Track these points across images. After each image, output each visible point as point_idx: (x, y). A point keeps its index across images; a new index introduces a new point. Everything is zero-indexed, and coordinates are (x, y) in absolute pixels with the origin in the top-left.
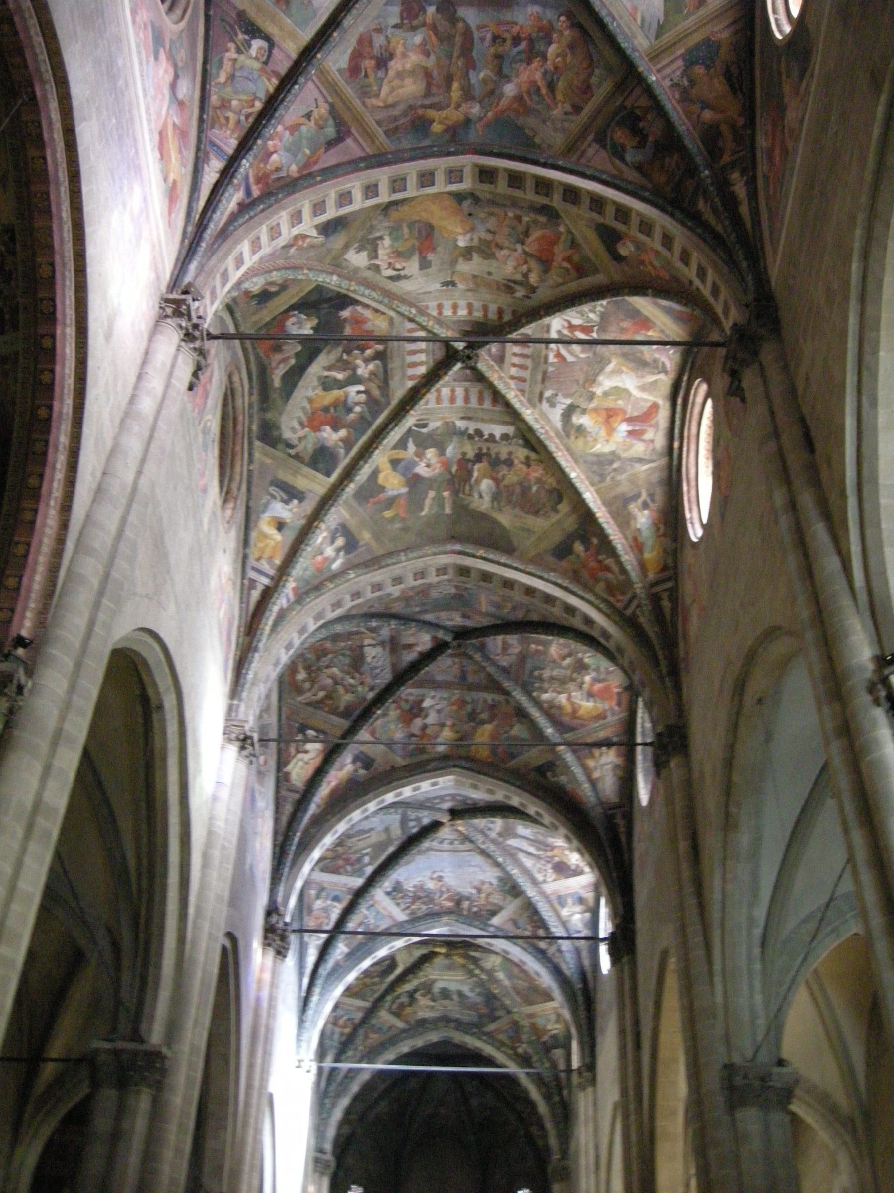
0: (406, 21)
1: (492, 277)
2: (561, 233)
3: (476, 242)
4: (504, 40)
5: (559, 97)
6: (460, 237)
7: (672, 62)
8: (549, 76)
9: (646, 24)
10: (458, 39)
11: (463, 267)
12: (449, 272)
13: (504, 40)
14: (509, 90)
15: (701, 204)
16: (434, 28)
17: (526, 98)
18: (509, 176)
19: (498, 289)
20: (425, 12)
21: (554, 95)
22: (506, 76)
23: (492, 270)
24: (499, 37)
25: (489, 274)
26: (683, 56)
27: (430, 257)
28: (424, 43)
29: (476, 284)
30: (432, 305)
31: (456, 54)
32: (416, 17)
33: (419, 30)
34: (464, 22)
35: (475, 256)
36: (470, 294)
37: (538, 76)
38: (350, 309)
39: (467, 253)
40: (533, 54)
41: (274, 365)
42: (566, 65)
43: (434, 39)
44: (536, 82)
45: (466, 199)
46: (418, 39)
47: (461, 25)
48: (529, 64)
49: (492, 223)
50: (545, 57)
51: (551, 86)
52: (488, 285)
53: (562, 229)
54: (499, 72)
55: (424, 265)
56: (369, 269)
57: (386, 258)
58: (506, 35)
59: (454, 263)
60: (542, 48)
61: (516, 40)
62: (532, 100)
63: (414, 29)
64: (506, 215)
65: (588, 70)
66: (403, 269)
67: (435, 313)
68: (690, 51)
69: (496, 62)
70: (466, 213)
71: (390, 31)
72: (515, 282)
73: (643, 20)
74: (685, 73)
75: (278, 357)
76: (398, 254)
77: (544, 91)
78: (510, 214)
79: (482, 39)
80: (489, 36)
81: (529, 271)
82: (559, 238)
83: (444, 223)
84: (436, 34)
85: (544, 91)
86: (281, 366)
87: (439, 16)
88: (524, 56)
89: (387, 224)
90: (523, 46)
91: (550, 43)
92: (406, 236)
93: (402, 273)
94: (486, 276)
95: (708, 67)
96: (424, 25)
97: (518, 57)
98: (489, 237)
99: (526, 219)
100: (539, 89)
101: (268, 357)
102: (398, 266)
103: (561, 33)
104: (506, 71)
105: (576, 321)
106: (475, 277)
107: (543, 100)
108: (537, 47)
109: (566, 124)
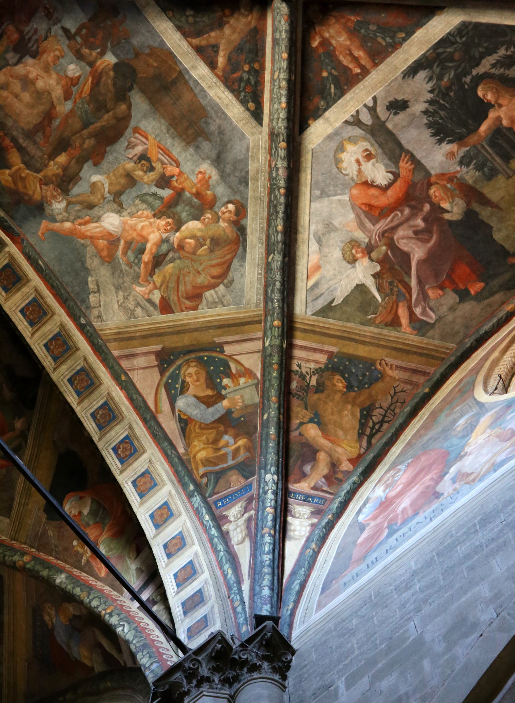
0: (79, 40)
4: (152, 169)
5: (157, 278)
7: (315, 350)
8: (164, 248)
9: (317, 292)
10: (107, 119)
13: (152, 169)
14: (111, 221)
15: (234, 512)
16: (97, 78)
17: (122, 243)
18: (35, 300)
20: (102, 54)
21: (152, 274)
22: (121, 205)
24: (149, 160)
26: (331, 355)
28: (74, 82)
31: (92, 128)
32: (91, 47)
33: (83, 64)
34: (129, 107)
37: (154, 237)
40: (169, 209)
42: (194, 253)
43: (87, 88)
44: (146, 241)
46: (73, 69)
47: (124, 107)
48: (154, 216)
50: (178, 225)
51: (158, 261)
54: (117, 195)
58: (158, 166)
60: (184, 215)
61: (164, 181)
62: (125, 253)
63: (80, 56)
65: (213, 281)
68: (342, 356)
69: (123, 181)
71: (56, 29)
73: (316, 285)
74: (318, 371)
77: (146, 257)
79: (131, 146)
80: (139, 149)
84: (92, 89)
85: (146, 257)
87: (112, 73)
88: (157, 204)
90: (166, 193)
91: (196, 218)
95: (349, 387)
96: (91, 64)
97: (150, 199)
100: (142, 251)
103: (217, 219)
104: (124, 198)
107: (138, 264)
108: (179, 208)
109: (139, 310)
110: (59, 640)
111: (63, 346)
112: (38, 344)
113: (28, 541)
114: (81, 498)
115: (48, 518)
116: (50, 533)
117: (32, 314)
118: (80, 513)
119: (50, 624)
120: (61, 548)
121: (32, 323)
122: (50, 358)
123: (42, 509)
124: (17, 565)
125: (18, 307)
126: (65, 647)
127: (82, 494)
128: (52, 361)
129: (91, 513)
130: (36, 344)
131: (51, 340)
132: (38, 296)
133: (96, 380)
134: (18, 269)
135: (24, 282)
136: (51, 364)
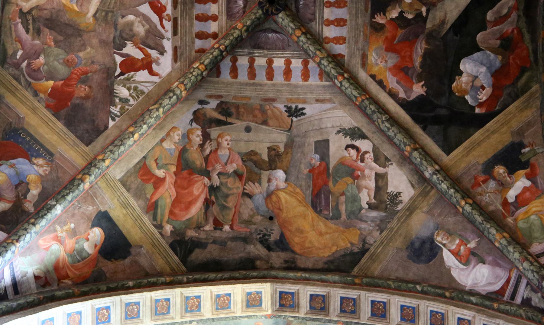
1: (244, 124)
2: (168, 222)
3: (265, 174)
6: (282, 185)
11: (279, 138)
12: (294, 131)
19: (237, 107)
23: (244, 135)
25: (248, 130)
27: (316, 159)
29: (263, 112)
30: (314, 80)
35: (265, 157)
36: (270, 95)
38: (413, 96)
39: (275, 159)
41: (514, 15)
45: (276, 242)
49: (247, 208)
52: (250, 110)
53: (168, 228)
55: (323, 147)
56: (387, 159)
57: (367, 172)
59: (290, 145)
64: (231, 228)
66: (348, 147)
67: (312, 65)
70: (275, 220)
72: (219, 123)
75: (507, 27)
76: (352, 172)
78: (227, 228)
81: (202, 146)
82: (171, 213)
83: (301, 209)
86: (505, 11)
89: (363, 226)
92: (343, 198)
93: (348, 141)
94: (252, 125)
98: (251, 187)
99: (208, 227)
101: (520, 32)
102: (353, 152)
105: (142, 75)
106: (265, 123)
110: (21, 160)
111: (191, 309)
112: (203, 293)
113: (96, 186)
114: (96, 246)
115: (100, 211)
116: (91, 208)
117: (222, 301)
118: (88, 240)
119: (35, 161)
120: (76, 211)
121: (218, 296)
122: (190, 295)
123: (108, 211)
124: (87, 176)
125: (234, 294)
126: (13, 161)
127: (98, 248)
128: (187, 295)
129: (83, 249)
130: (205, 291)
131: (199, 303)
132: (230, 311)
133: (157, 317)
134: (254, 310)
135: (244, 308)
136: (186, 293)
